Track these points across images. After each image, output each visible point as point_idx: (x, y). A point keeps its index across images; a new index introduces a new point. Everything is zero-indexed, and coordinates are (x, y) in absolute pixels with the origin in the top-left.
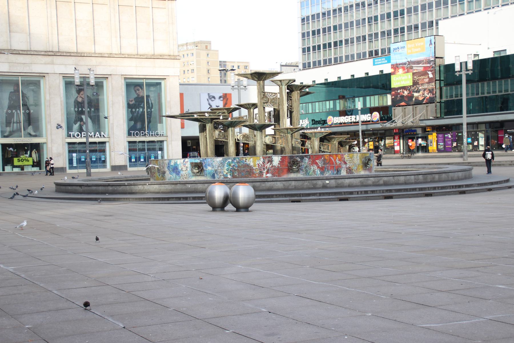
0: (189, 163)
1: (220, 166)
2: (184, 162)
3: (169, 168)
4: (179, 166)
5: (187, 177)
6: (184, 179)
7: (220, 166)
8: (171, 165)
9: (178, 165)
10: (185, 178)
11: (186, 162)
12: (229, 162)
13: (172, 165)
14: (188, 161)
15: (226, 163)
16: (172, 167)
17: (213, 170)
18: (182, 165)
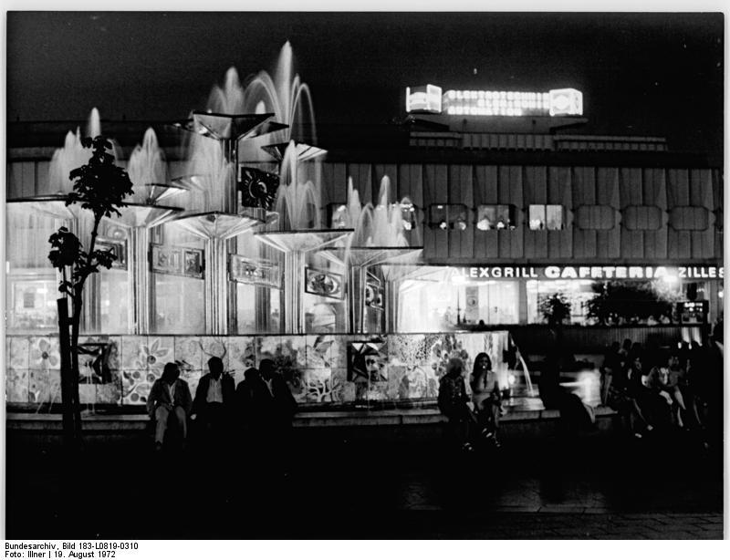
0: (335, 346)
1: (420, 355)
2: (319, 345)
3: (250, 361)
4: (299, 354)
5: (329, 388)
6: (318, 392)
7: (420, 355)
8: (263, 350)
9: (295, 353)
10: (321, 390)
11: (328, 343)
12: (437, 345)
13: (267, 353)
14: (332, 342)
15: (432, 348)
16: (264, 357)
17: (404, 367)
18: (310, 353)
